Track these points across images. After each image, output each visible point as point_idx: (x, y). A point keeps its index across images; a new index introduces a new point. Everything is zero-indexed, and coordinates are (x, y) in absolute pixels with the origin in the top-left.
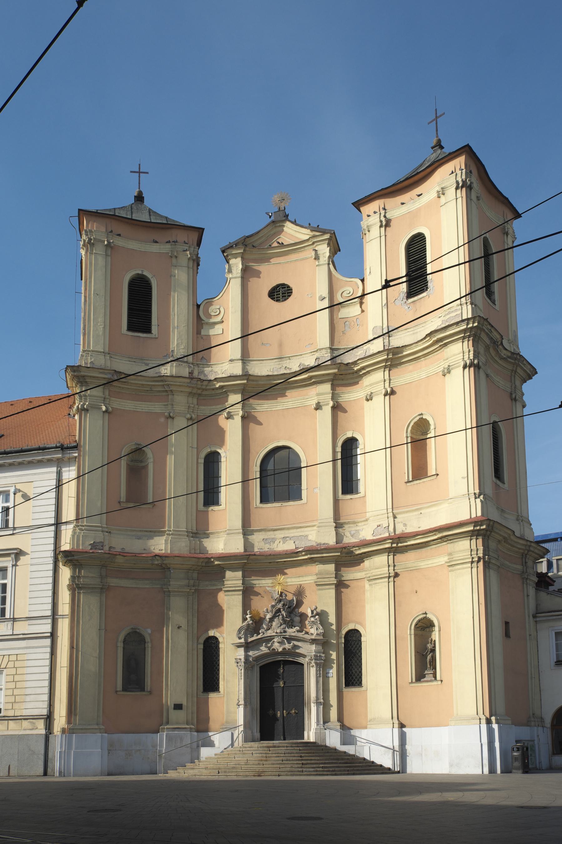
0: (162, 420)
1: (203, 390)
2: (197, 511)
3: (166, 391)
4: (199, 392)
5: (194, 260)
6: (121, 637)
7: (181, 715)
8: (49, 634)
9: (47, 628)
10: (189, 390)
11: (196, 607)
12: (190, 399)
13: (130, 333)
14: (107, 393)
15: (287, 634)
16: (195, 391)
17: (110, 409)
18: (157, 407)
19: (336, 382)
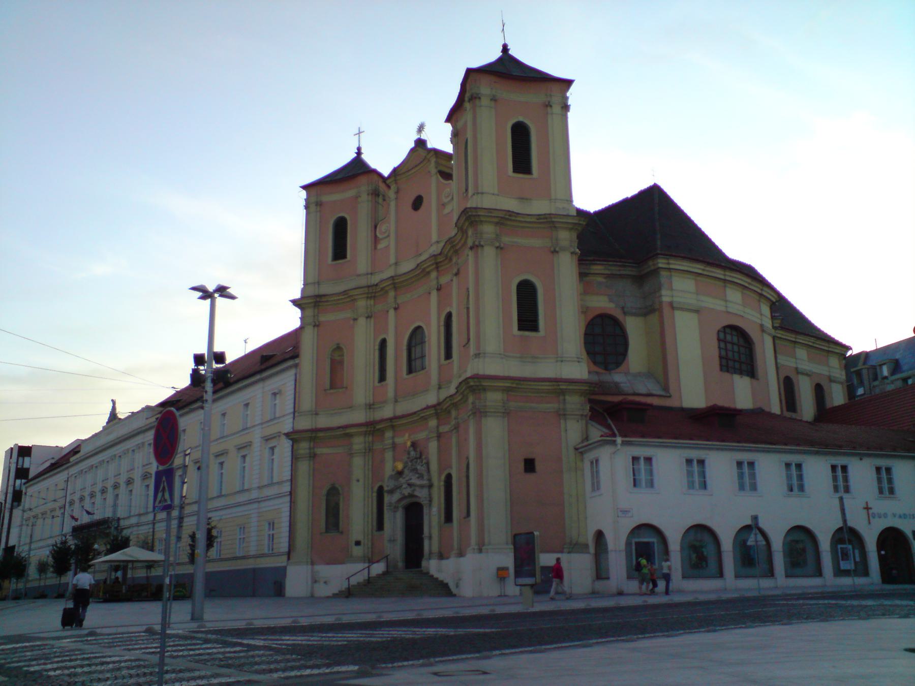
0: (352, 322)
1: (375, 292)
2: (374, 388)
3: (352, 300)
4: (373, 295)
5: (372, 194)
6: (324, 492)
7: (358, 548)
8: (288, 493)
9: (288, 489)
10: (366, 296)
11: (370, 463)
12: (369, 302)
13: (335, 262)
14: (316, 310)
15: (410, 481)
16: (370, 296)
17: (317, 323)
18: (348, 314)
19: (440, 269)
